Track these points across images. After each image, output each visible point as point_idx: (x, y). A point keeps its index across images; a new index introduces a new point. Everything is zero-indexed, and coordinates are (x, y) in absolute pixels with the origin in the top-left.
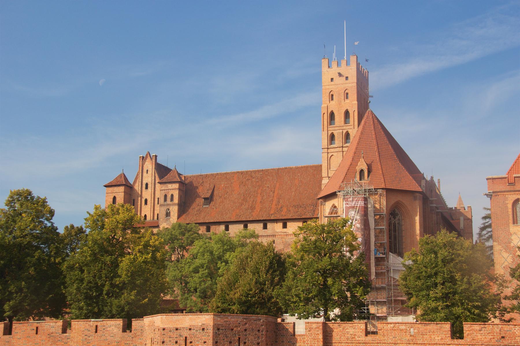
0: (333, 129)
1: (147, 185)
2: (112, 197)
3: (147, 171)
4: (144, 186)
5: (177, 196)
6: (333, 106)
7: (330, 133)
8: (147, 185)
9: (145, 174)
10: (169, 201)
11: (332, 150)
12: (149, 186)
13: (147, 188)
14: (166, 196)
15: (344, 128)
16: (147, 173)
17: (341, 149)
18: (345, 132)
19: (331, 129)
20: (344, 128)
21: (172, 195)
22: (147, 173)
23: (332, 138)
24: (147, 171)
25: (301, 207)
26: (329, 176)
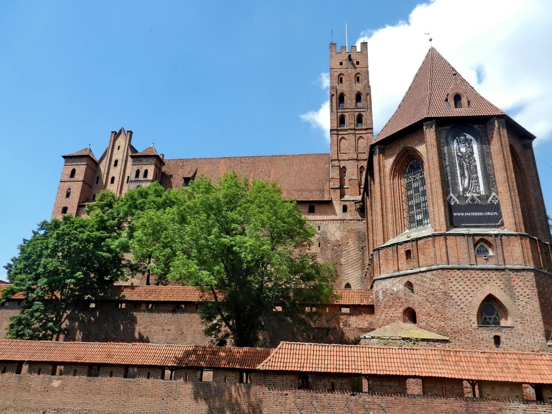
0: (343, 111)
1: (116, 162)
2: (71, 169)
3: (119, 147)
4: (113, 163)
5: (152, 172)
6: (343, 88)
7: (339, 114)
8: (116, 162)
9: (116, 150)
10: (141, 177)
11: (342, 133)
12: (119, 163)
13: (116, 165)
14: (138, 172)
15: (356, 110)
16: (119, 149)
17: (353, 132)
18: (356, 114)
19: (340, 110)
20: (356, 110)
21: (146, 172)
22: (119, 149)
23: (342, 120)
24: (119, 147)
25: (304, 191)
26: (340, 158)
